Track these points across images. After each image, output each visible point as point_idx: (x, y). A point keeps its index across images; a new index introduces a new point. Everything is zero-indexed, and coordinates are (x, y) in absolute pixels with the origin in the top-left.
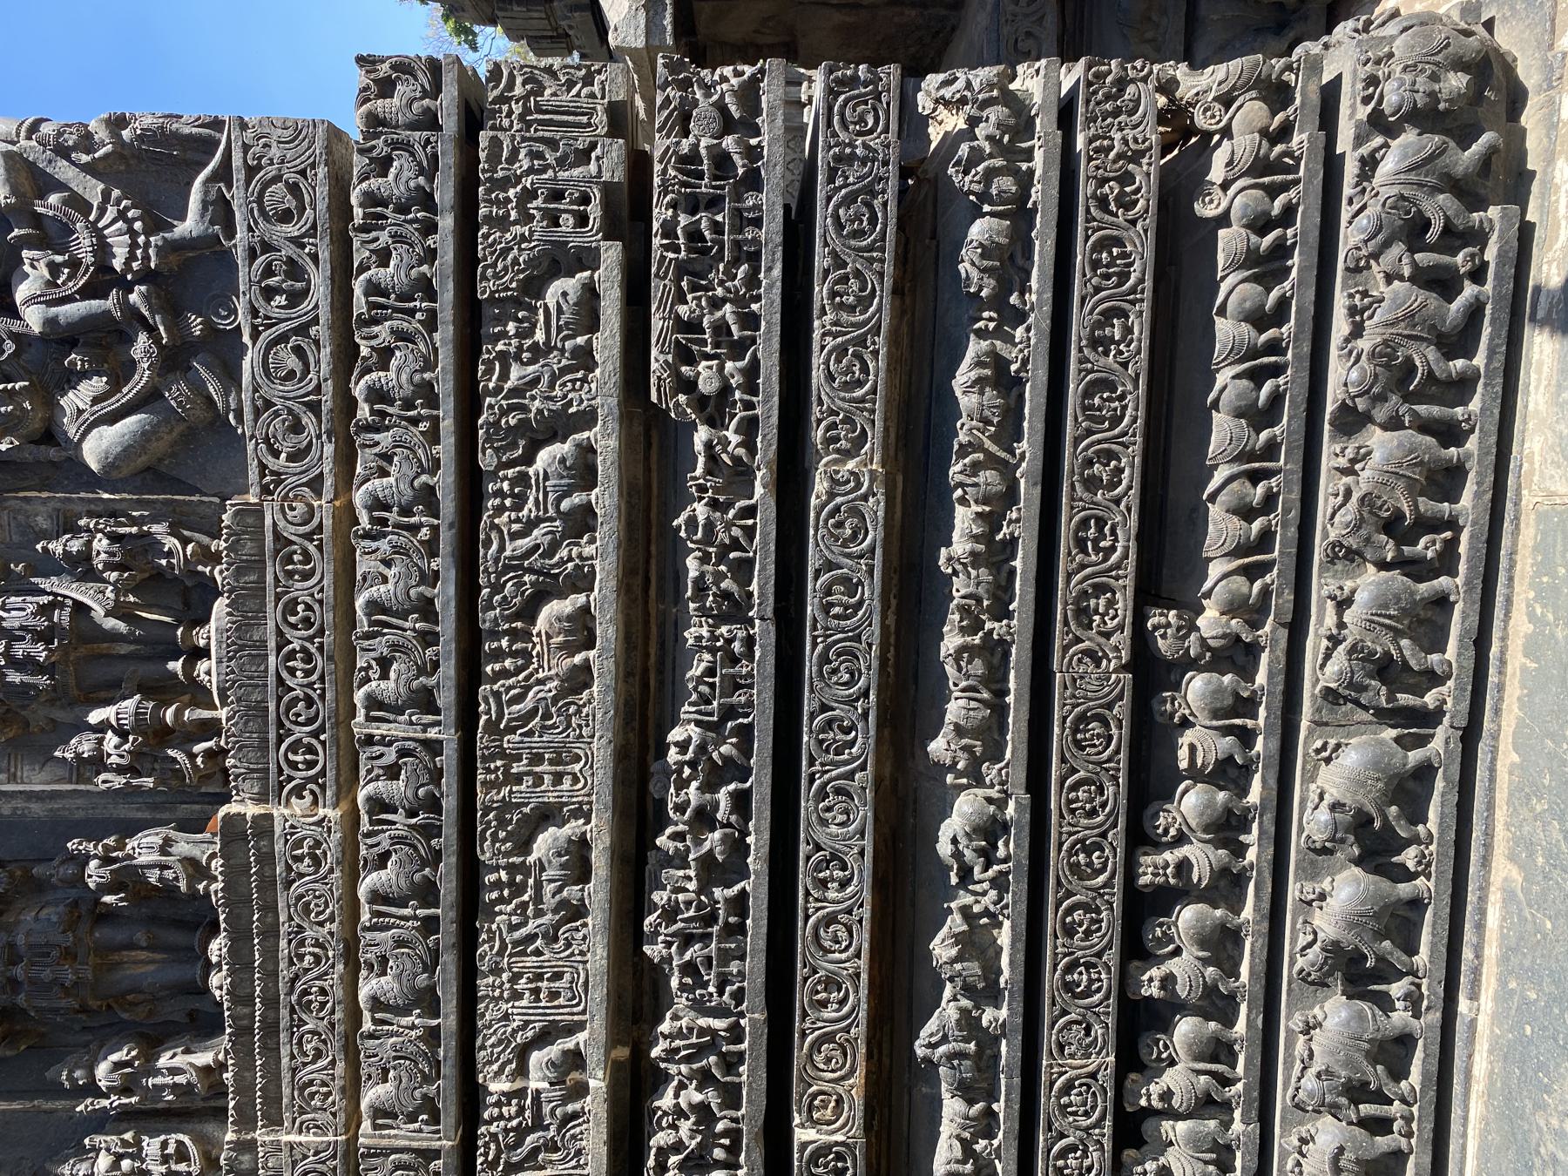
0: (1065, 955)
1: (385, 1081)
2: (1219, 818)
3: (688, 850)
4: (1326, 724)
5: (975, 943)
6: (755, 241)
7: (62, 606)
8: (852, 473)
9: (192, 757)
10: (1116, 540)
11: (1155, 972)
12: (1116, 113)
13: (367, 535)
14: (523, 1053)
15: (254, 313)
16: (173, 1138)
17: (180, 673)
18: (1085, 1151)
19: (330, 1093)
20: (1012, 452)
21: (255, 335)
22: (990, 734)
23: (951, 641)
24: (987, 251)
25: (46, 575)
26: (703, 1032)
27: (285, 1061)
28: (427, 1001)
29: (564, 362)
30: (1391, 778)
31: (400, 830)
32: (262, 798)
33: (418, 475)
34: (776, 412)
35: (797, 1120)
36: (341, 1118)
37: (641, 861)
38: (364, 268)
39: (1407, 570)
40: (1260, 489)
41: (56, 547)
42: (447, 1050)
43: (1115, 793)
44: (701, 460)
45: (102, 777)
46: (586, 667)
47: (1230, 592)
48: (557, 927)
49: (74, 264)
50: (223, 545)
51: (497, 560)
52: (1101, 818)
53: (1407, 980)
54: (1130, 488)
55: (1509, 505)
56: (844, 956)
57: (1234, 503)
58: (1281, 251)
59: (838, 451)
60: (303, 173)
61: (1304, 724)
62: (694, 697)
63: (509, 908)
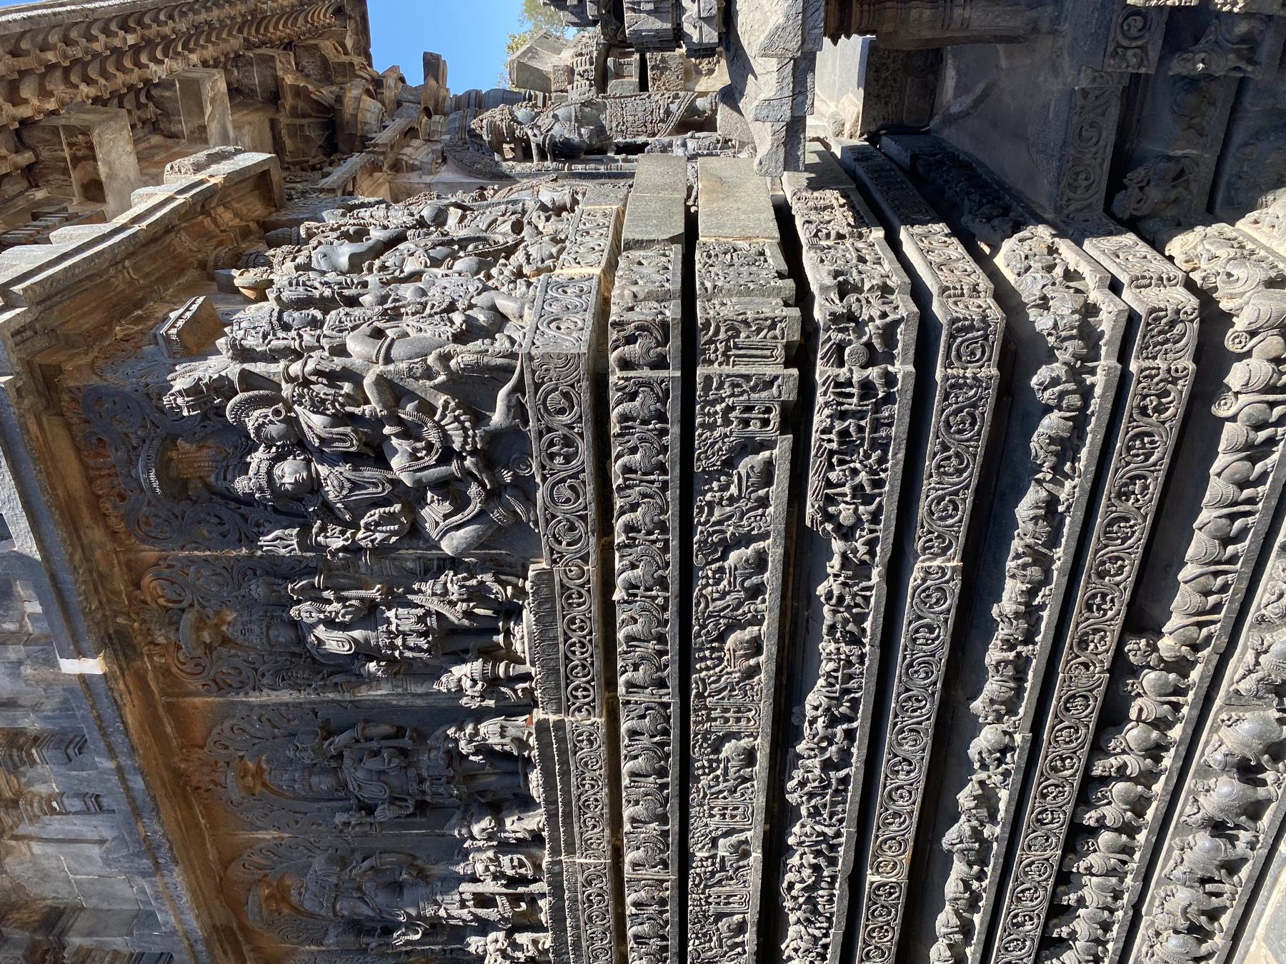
5: (987, 799)
6: (889, 437)
8: (940, 567)
9: (515, 691)
12: (1166, 341)
14: (714, 842)
15: (544, 468)
16: (515, 857)
18: (1036, 891)
21: (544, 479)
23: (993, 655)
24: (1052, 440)
26: (819, 834)
28: (663, 819)
29: (750, 505)
32: (558, 711)
34: (892, 536)
35: (869, 871)
38: (619, 456)
40: (1220, 581)
49: (430, 447)
51: (703, 613)
52: (1074, 744)
57: (1199, 589)
58: (1271, 442)
60: (572, 386)
61: (1218, 702)
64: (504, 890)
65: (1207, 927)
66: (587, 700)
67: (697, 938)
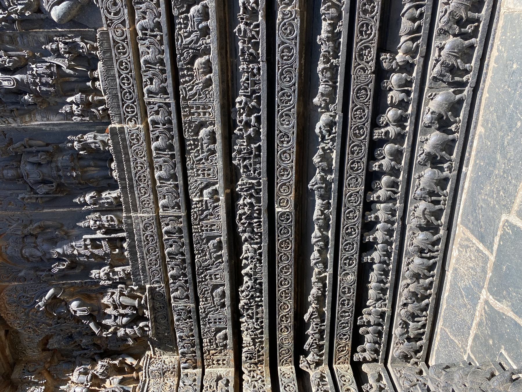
0: (351, 159)
1: (165, 199)
2: (398, 118)
3: (243, 134)
4: (433, 88)
5: (326, 157)
7: (53, 66)
8: (289, 11)
9: (99, 111)
10: (372, 31)
11: (377, 164)
13: (142, 39)
14: (201, 191)
16: (109, 216)
17: (91, 86)
19: (149, 203)
20: (341, 3)
22: (331, 96)
23: (321, 66)
25: (47, 57)
26: (250, 184)
27: (136, 195)
28: (174, 177)
30: (450, 103)
31: (161, 129)
32: (120, 122)
33: (155, 18)
35: (276, 206)
36: (154, 210)
37: (230, 138)
39: (462, 36)
40: (418, 11)
41: (48, 47)
42: (181, 190)
43: (368, 112)
44: (242, 9)
45: (74, 118)
46: (210, 79)
47: (406, 47)
48: (208, 156)
50: (98, 44)
51: (181, 45)
52: (364, 119)
53: (449, 163)
54: (377, 13)
55: (497, 13)
56: (288, 162)
57: (409, 17)
59: (285, 4)
61: (426, 88)
62: (243, 87)
63: (194, 151)
64: (105, 236)
65: (435, 223)
66: (133, 114)
67: (199, 254)
